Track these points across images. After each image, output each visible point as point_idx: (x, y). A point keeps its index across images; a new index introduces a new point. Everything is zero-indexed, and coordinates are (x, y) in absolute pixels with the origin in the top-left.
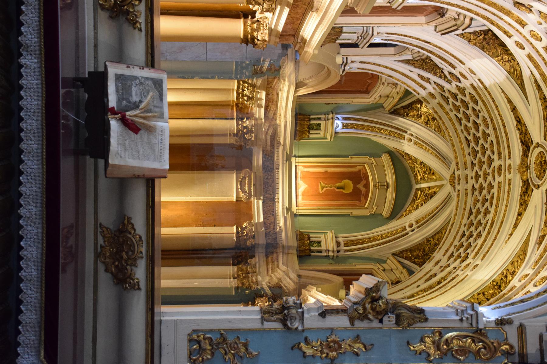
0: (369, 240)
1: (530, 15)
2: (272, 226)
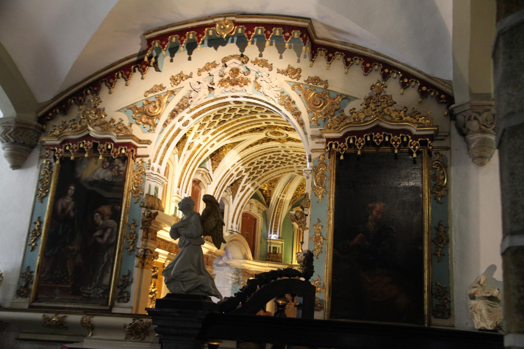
1: (195, 143)
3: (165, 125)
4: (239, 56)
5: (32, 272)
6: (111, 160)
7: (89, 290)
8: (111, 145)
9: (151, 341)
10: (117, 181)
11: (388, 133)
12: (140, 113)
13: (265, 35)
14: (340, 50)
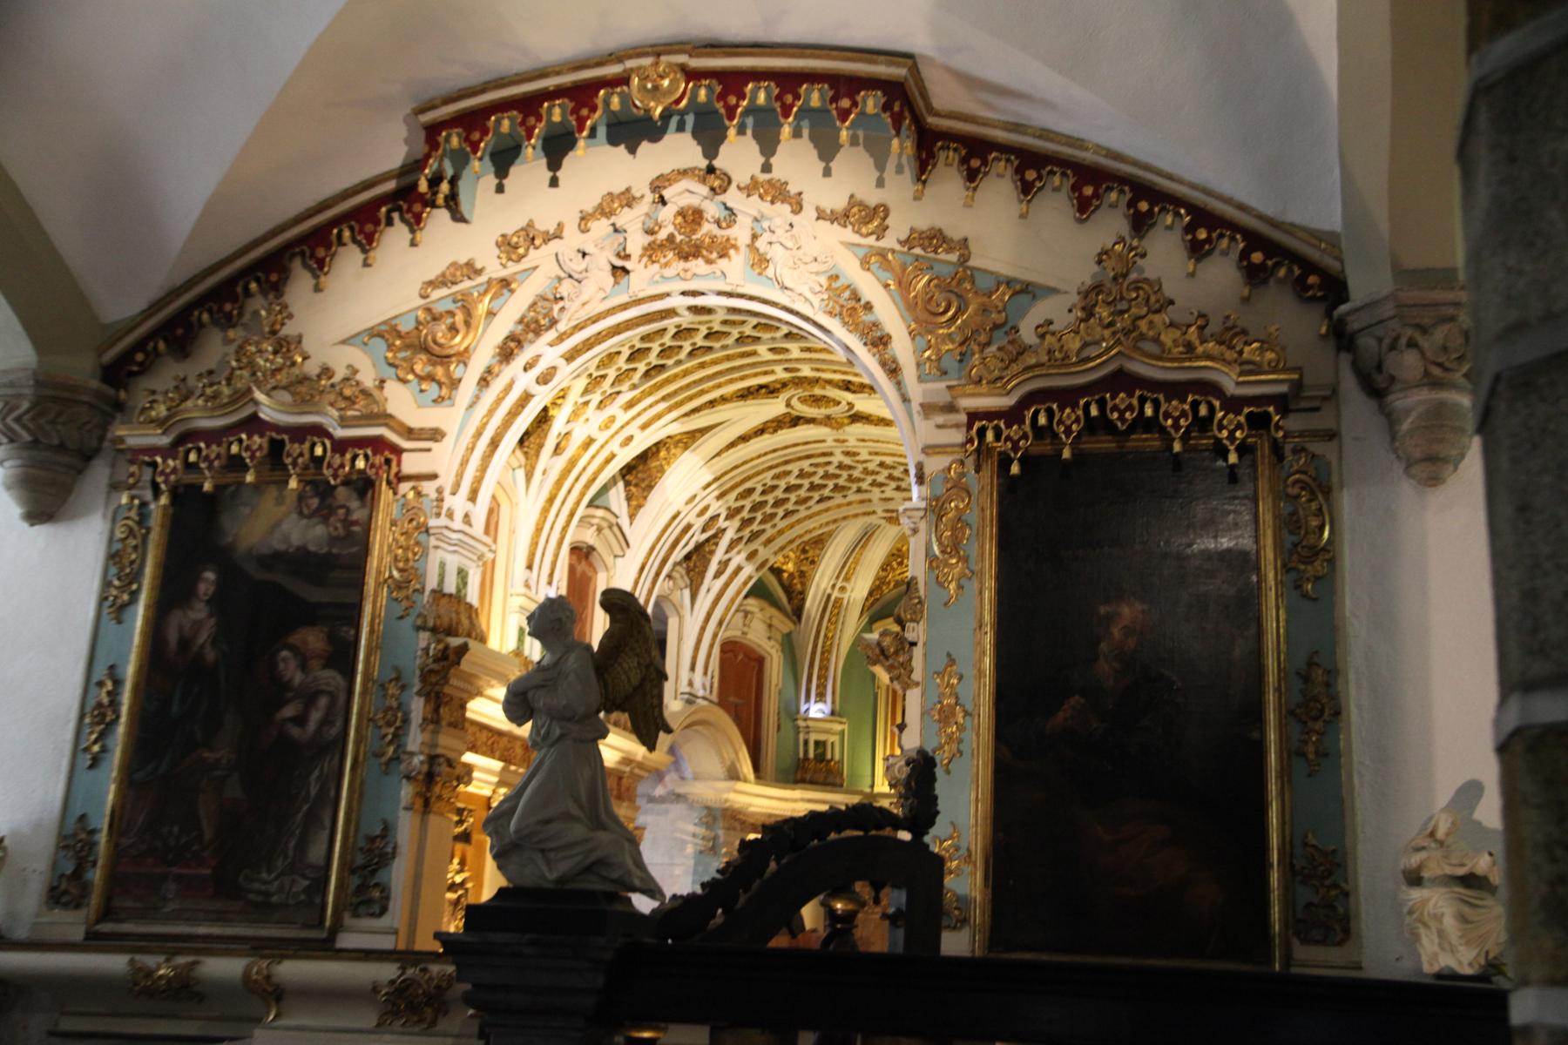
3: (484, 382)
4: (700, 170)
5: (93, 832)
6: (324, 491)
7: (265, 883)
8: (324, 445)
10: (345, 552)
11: (1153, 392)
12: (407, 347)
13: (777, 106)
14: (1005, 149)
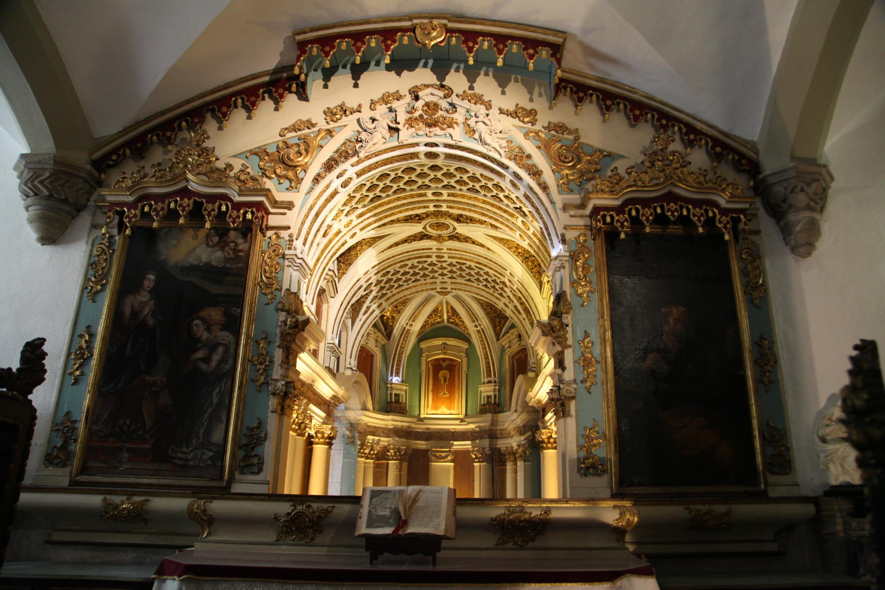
0: (487, 358)
1: (334, 226)
2: (475, 434)
3: (316, 180)
4: (437, 85)
5: (75, 422)
7: (185, 453)
9: (328, 542)
10: (234, 267)
12: (271, 161)
14: (595, 89)
